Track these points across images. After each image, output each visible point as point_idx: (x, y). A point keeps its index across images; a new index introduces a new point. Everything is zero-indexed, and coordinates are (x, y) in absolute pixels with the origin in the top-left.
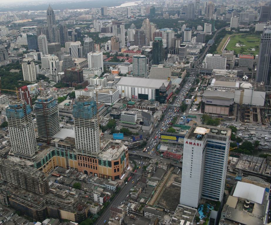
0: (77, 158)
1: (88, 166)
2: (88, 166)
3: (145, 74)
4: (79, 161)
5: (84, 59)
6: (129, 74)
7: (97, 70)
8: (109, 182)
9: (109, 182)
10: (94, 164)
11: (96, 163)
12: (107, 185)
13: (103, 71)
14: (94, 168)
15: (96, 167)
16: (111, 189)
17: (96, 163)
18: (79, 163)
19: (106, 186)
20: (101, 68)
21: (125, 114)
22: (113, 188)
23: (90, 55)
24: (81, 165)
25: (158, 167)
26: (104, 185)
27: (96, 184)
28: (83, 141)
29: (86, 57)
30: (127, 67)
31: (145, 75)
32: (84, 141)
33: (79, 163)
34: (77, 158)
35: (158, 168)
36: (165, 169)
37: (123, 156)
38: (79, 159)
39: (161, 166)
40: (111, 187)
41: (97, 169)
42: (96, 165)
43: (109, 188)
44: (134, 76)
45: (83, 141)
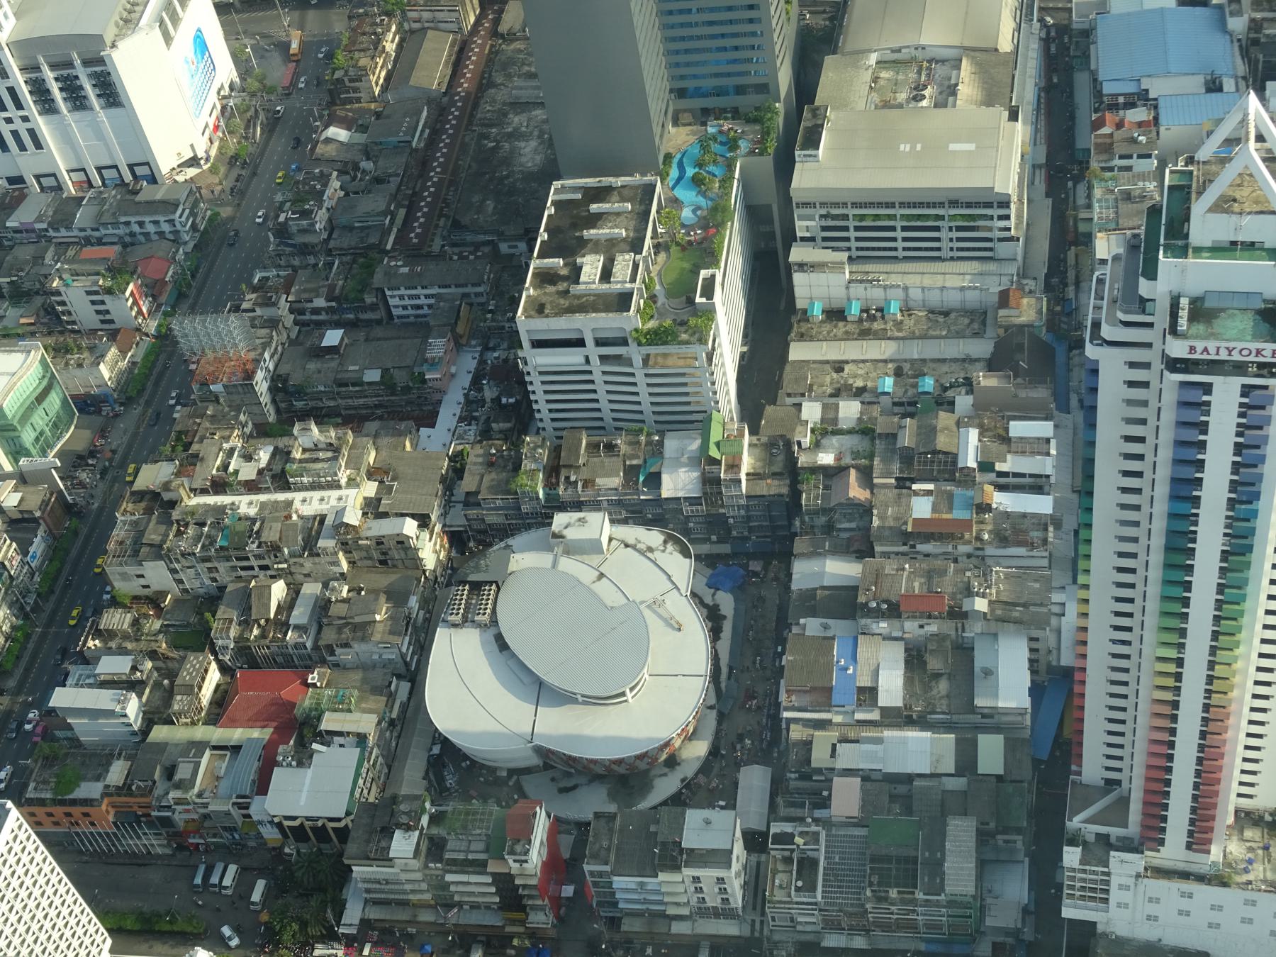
8: (139, 198)
9: (139, 198)
12: (133, 219)
14: (22, 148)
15: (32, 133)
16: (161, 234)
17: (19, 105)
19: (128, 224)
22: (171, 222)
25: (406, 26)
26: (116, 225)
27: (63, 232)
35: (412, 32)
37: (175, 20)
39: (426, 15)
40: (156, 223)
43: (151, 228)
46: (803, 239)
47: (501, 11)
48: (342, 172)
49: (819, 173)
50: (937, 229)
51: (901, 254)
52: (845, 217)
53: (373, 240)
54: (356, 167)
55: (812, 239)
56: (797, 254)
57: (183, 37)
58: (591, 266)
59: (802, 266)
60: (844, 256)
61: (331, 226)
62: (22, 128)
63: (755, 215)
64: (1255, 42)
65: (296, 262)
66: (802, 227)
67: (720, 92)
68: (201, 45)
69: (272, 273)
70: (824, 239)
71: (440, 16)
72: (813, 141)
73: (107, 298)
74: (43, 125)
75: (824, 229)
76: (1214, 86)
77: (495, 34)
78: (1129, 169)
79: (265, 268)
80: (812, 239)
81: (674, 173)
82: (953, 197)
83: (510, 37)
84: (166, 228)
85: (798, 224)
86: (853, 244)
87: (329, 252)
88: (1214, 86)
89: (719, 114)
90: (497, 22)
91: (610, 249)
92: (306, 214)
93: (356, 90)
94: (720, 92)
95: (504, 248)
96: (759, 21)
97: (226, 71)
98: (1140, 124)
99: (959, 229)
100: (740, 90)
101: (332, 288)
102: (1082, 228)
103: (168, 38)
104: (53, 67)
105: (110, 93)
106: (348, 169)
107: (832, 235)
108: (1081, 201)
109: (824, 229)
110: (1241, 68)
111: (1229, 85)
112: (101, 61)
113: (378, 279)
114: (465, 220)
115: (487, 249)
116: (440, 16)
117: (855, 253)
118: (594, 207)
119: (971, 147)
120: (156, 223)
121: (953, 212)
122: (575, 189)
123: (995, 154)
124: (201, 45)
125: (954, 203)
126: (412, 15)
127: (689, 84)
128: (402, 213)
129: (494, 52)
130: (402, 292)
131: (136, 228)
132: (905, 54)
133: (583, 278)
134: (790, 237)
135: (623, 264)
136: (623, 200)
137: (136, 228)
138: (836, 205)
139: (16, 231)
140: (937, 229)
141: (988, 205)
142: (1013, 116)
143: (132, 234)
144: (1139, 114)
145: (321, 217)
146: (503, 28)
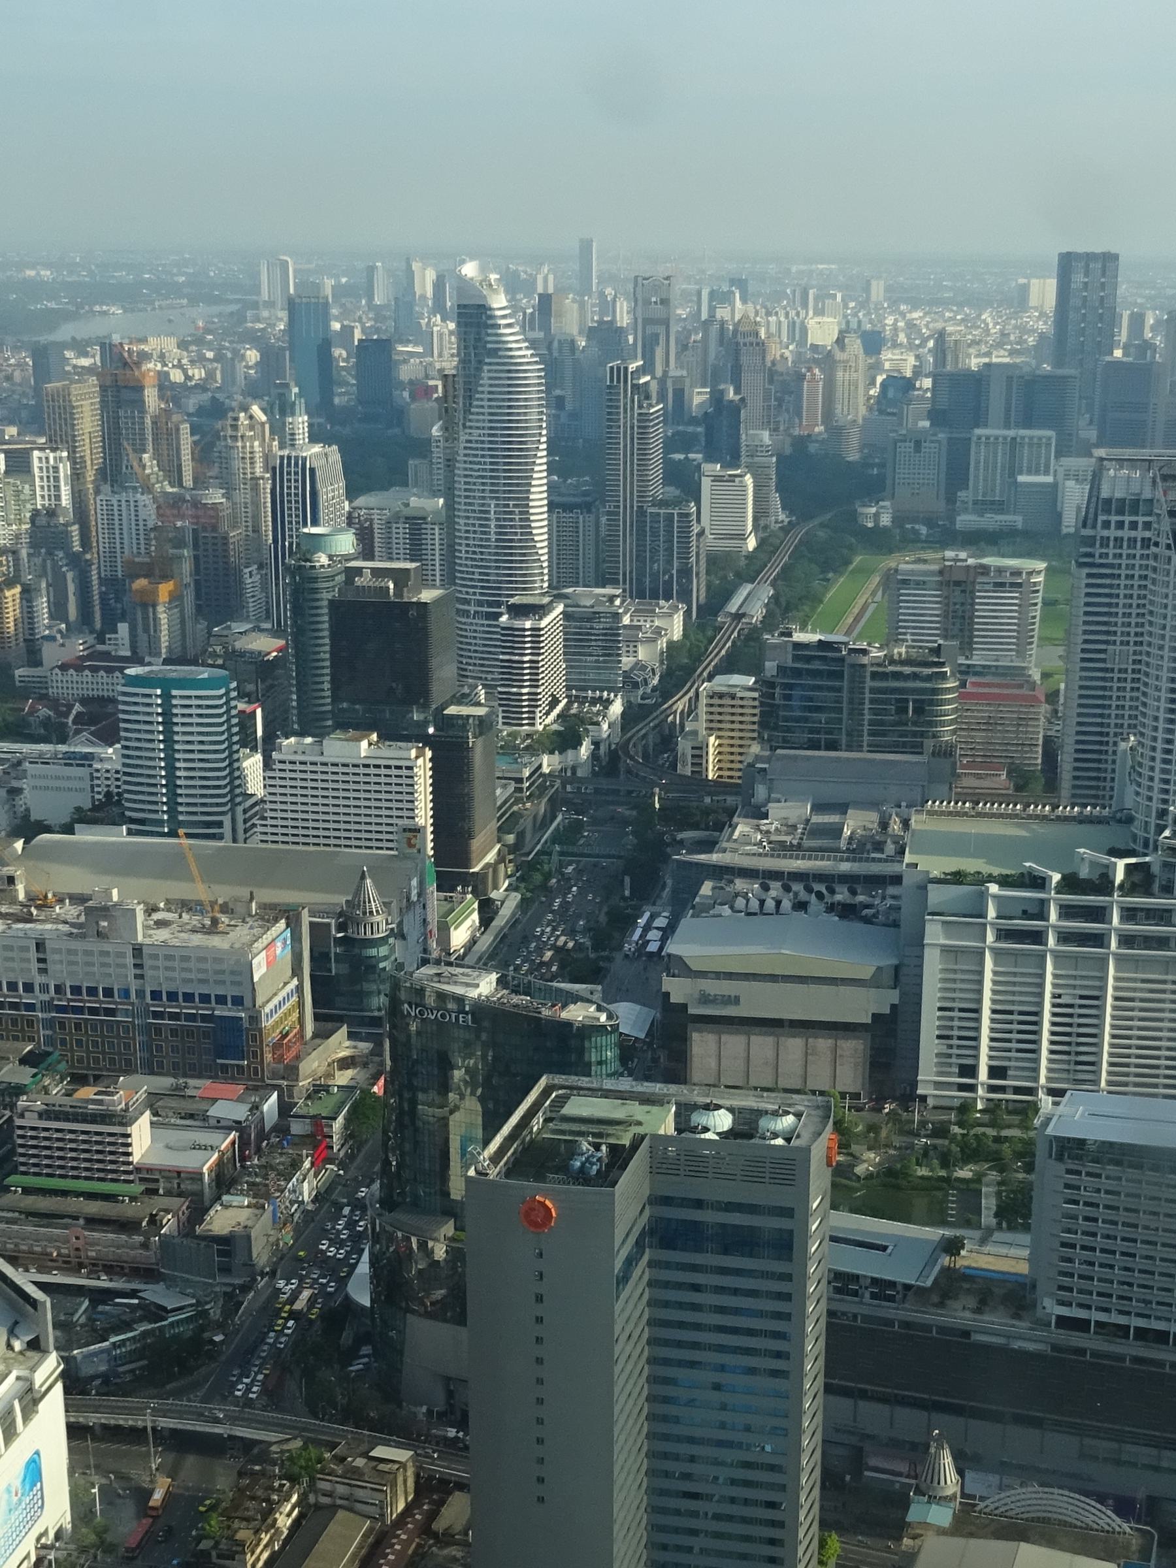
3: (227, 820)
21: (41, 1115)
25: (312, 1499)
35: (318, 1507)
39: (341, 1489)
47: (442, 1503)
71: (360, 1494)
77: (426, 1530)
83: (447, 1538)
90: (433, 1515)
96: (780, 1525)
97: (57, 1511)
126: (322, 1485)
129: (421, 1554)
146: (439, 1525)
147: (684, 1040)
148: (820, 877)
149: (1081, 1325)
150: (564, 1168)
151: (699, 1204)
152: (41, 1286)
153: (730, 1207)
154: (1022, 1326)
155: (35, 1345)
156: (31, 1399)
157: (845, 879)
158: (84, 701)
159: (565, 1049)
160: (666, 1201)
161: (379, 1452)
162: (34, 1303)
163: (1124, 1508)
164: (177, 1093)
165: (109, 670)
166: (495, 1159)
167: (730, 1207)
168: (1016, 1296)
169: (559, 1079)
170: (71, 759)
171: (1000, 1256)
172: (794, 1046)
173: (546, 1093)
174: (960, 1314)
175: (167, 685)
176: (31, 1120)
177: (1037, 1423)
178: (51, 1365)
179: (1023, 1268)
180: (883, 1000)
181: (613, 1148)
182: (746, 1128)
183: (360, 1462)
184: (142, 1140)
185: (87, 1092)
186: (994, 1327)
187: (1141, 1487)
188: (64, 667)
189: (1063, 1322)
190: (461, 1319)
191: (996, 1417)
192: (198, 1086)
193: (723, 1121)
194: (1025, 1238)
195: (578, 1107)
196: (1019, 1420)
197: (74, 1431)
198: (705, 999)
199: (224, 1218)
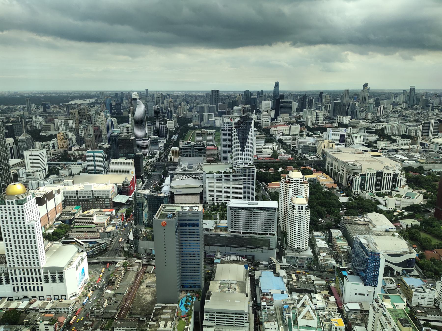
0: (11, 280)
1: (28, 289)
2: (28, 289)
4: (13, 284)
5: (20, 160)
6: (83, 172)
7: (40, 171)
10: (37, 284)
11: (41, 281)
13: (47, 173)
14: (38, 290)
15: (42, 287)
16: (65, 311)
17: (41, 281)
18: (14, 288)
20: (45, 169)
22: (68, 309)
23: (26, 154)
24: (18, 290)
27: (42, 310)
28: (19, 254)
29: (22, 157)
30: (81, 165)
31: (104, 173)
32: (20, 253)
33: (14, 288)
34: (11, 280)
36: (136, 270)
37: (79, 265)
38: (13, 281)
39: (131, 268)
40: (64, 309)
41: (42, 290)
42: (41, 284)
44: (90, 173)
45: (19, 254)
46: (205, 320)
48: (108, 300)
49: (208, 305)
50: (233, 319)
51: (225, 324)
52: (214, 315)
53: (113, 315)
54: (111, 299)
55: (207, 320)
56: (205, 323)
57: (80, 268)
58: (162, 324)
59: (205, 326)
60: (213, 324)
61: (104, 312)
62: (40, 285)
63: (196, 314)
64: (288, 284)
65: (94, 320)
66: (206, 317)
67: (191, 287)
68: (83, 270)
69: (88, 322)
70: (210, 320)
71: (134, 268)
72: (209, 299)
73: (49, 326)
74: (45, 285)
75: (210, 318)
76: (283, 292)
78: (269, 308)
79: (87, 321)
80: (207, 320)
81: (180, 303)
82: (236, 312)
84: (66, 310)
85: (205, 316)
86: (216, 322)
87: (102, 318)
88: (283, 292)
89: (190, 291)
91: (166, 320)
92: (99, 309)
93: (114, 282)
94: (191, 287)
95: (141, 319)
97: (87, 276)
98: (270, 299)
99: (237, 319)
100: (195, 286)
101: (102, 326)
102: (261, 321)
103: (77, 268)
104: (51, 273)
105: (61, 279)
106: (110, 299)
107: (211, 319)
108: (259, 315)
109: (210, 318)
110: (287, 290)
111: (285, 292)
112: (62, 273)
113: (113, 325)
114: (133, 312)
115: (137, 319)
116: (134, 268)
117: (216, 324)
118: (164, 311)
119: (239, 301)
120: (64, 309)
121: (236, 315)
122: (160, 306)
123: (243, 304)
124: (83, 270)
125: (236, 314)
127: (184, 285)
128: (120, 309)
130: (118, 328)
131: (59, 310)
132: (226, 282)
133: (160, 327)
134: (203, 319)
135: (169, 324)
136: (170, 309)
137: (59, 310)
138: (212, 312)
139: (31, 309)
140: (233, 319)
141: (243, 314)
142: (247, 296)
143: (58, 311)
144: (269, 297)
145: (102, 309)
147: (174, 198)
148: (190, 174)
149: (234, 232)
150: (167, 217)
151: (186, 220)
152: (83, 242)
153: (189, 220)
154: (227, 233)
155: (82, 251)
156: (82, 260)
157: (194, 174)
158: (79, 155)
159: (161, 200)
160: (181, 220)
161: (137, 261)
162: (82, 245)
163: (242, 257)
164: (100, 211)
165: (83, 151)
166: (157, 217)
167: (189, 220)
168: (225, 229)
169: (164, 204)
170: (78, 164)
171: (223, 223)
172: (189, 197)
173: (162, 207)
174: (218, 232)
175: (94, 152)
176: (77, 217)
177: (230, 246)
178: (85, 254)
179: (226, 225)
180: (201, 190)
181: (174, 214)
182: (191, 209)
183: (134, 263)
184: (96, 219)
185: (85, 213)
186: (223, 234)
187: (244, 254)
188: (75, 150)
189: (232, 232)
190: (153, 241)
191: (224, 246)
192: (103, 210)
193: (188, 208)
194: (226, 221)
195: (167, 208)
196: (227, 246)
197: (89, 264)
198: (177, 192)
199: (109, 229)
